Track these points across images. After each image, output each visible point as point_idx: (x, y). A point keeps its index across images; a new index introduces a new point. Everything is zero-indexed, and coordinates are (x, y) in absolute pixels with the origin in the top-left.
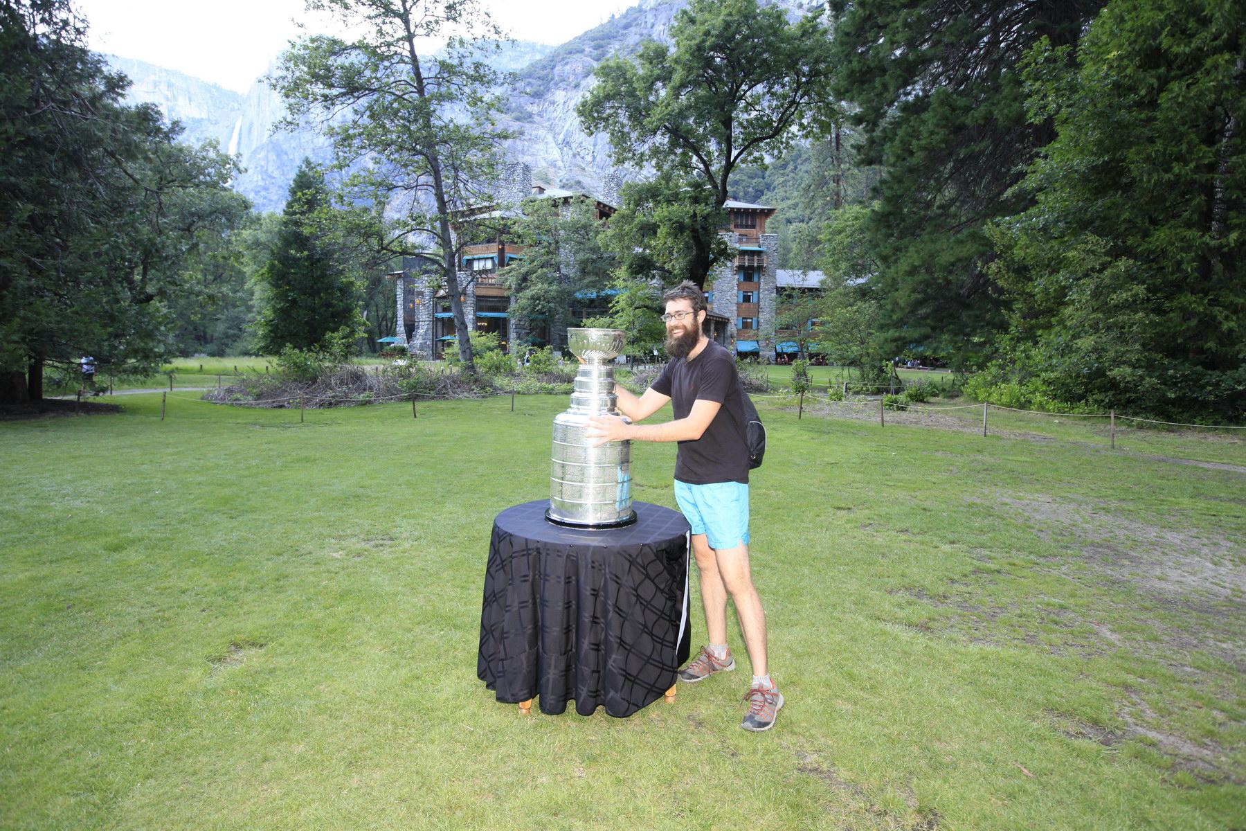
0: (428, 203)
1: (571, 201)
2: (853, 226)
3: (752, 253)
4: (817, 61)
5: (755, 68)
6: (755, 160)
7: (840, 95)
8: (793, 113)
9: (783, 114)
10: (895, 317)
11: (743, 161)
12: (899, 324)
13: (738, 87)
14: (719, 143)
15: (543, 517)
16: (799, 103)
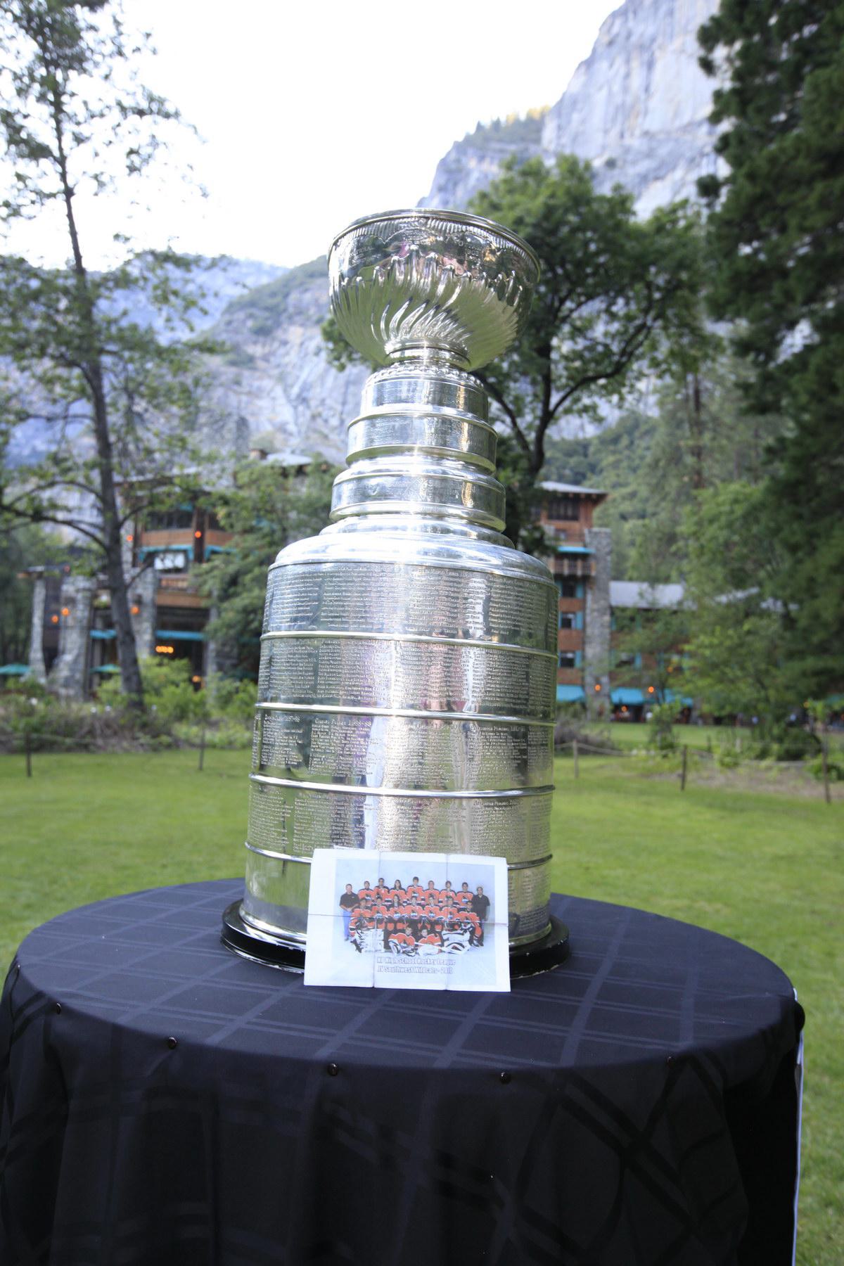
0: (83, 444)
1: (308, 469)
2: (732, 512)
3: (574, 556)
4: (681, 265)
5: (587, 276)
6: (586, 409)
7: (719, 312)
8: (641, 344)
9: (628, 342)
10: (815, 639)
11: (568, 411)
12: (823, 649)
13: (562, 302)
14: (534, 383)
15: (217, 930)
16: (649, 329)
